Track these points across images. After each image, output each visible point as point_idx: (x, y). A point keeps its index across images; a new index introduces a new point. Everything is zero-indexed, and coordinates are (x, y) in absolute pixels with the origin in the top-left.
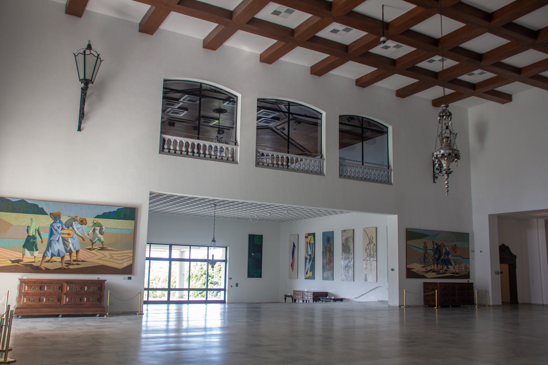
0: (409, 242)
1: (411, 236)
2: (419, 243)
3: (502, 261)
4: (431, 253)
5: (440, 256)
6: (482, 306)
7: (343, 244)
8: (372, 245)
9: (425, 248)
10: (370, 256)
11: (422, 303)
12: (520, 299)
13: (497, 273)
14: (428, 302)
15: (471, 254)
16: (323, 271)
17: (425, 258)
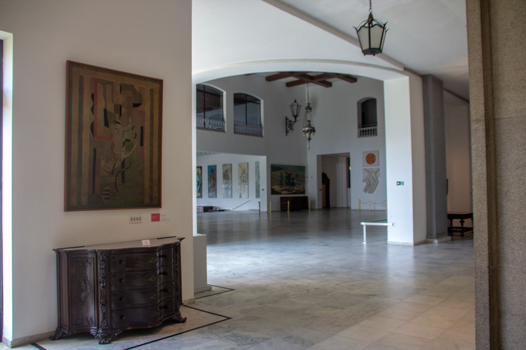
0: (273, 173)
1: (274, 168)
2: (278, 173)
3: (323, 183)
4: (285, 179)
5: (289, 180)
6: (312, 210)
7: (224, 174)
8: (245, 174)
9: (282, 176)
10: (243, 181)
11: (279, 208)
12: (331, 205)
13: (320, 190)
14: (283, 209)
15: (306, 179)
16: (209, 191)
17: (281, 182)
